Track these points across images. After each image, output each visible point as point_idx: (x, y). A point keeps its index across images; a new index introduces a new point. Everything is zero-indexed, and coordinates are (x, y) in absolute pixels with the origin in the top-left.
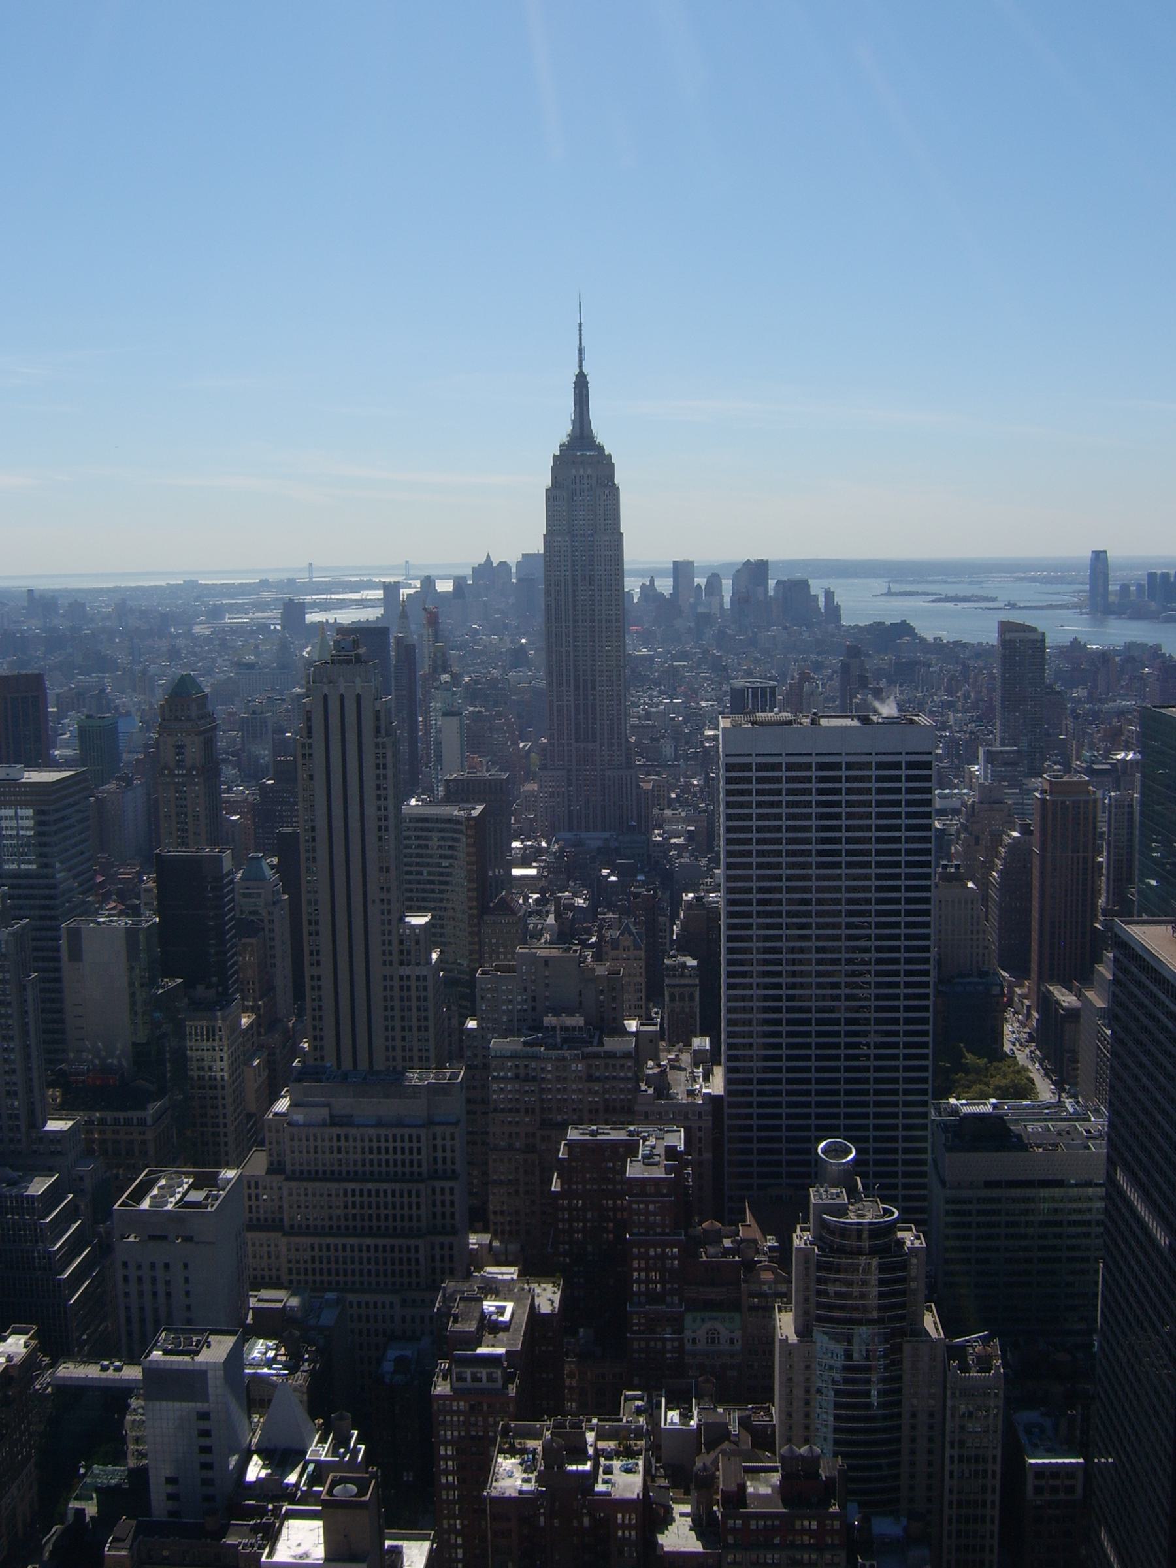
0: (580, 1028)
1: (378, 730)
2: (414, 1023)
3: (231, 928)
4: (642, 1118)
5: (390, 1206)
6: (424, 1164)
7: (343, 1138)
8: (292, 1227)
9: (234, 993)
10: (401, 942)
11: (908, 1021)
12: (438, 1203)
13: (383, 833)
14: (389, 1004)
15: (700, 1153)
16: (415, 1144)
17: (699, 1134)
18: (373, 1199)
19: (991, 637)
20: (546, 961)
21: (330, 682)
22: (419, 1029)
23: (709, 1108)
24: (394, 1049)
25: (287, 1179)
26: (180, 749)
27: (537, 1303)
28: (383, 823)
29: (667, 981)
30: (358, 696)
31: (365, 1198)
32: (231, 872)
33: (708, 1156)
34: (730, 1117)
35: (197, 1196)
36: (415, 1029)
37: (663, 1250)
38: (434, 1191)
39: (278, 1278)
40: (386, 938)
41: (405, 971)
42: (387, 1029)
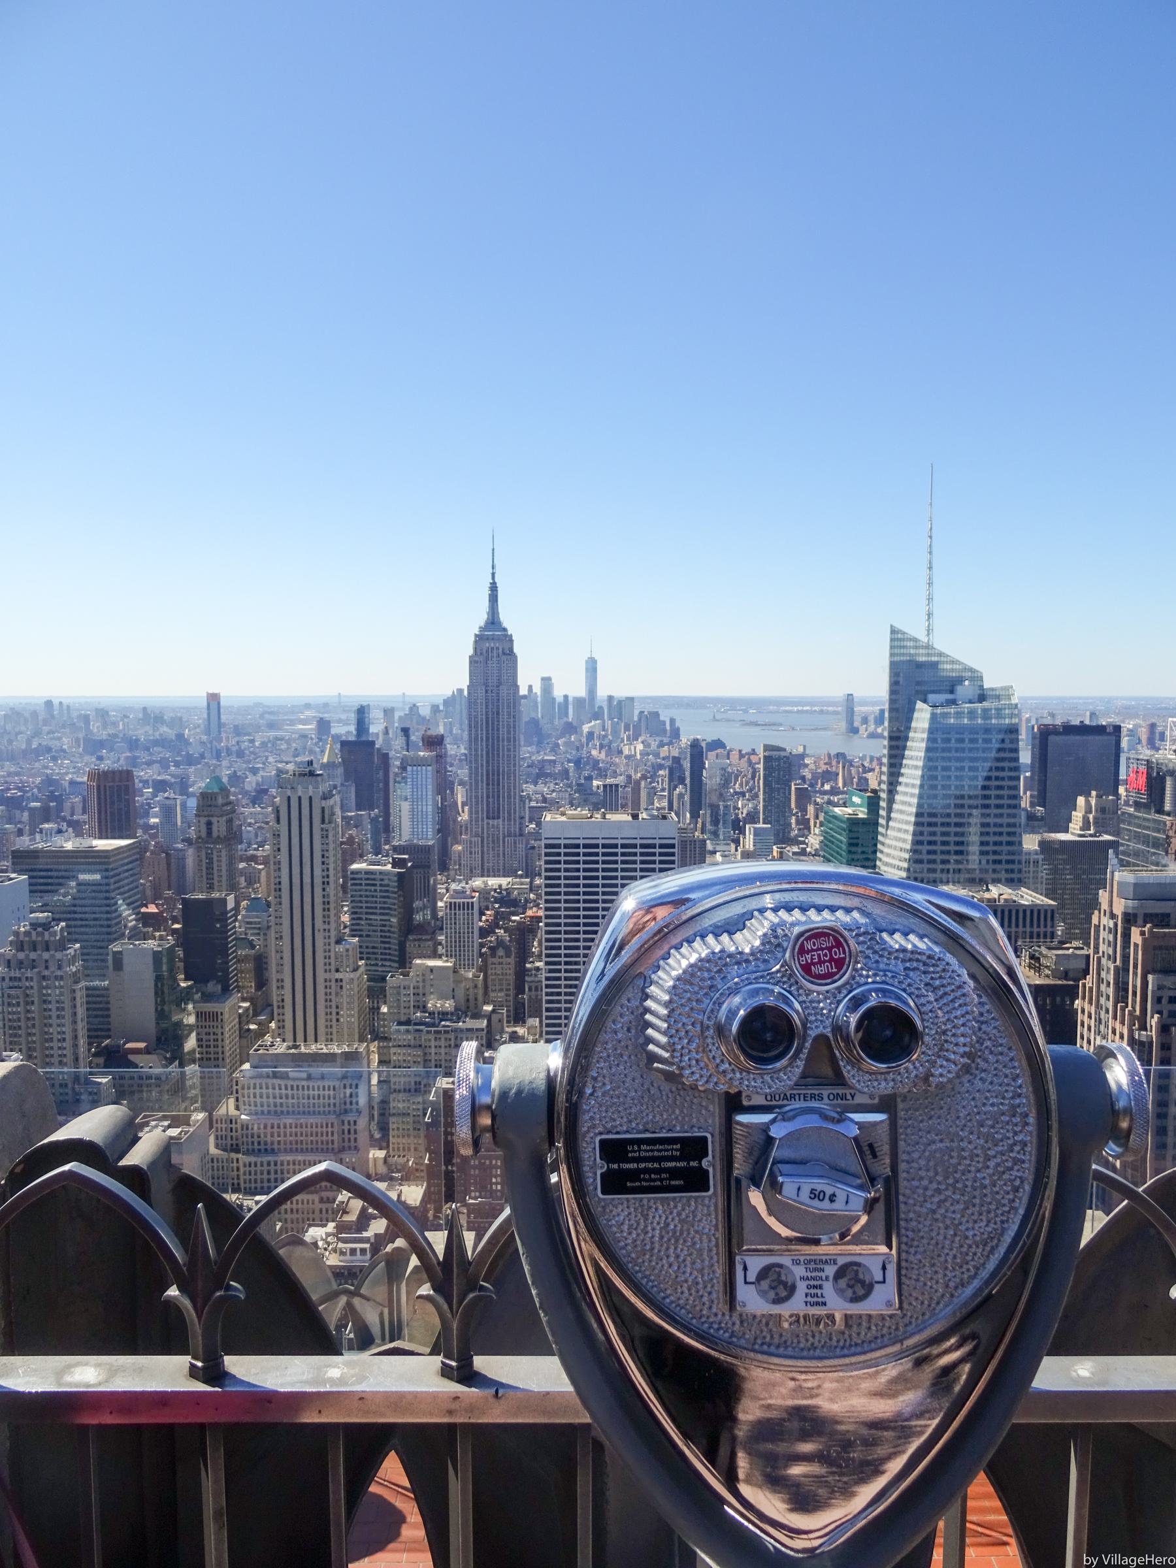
0: (452, 1014)
1: (323, 822)
3: (232, 947)
6: (337, 1105)
7: (283, 1087)
9: (233, 989)
13: (326, 886)
14: (328, 997)
20: (432, 970)
21: (292, 788)
24: (331, 1027)
26: (209, 824)
27: (403, 1199)
28: (326, 880)
29: (527, 978)
30: (311, 798)
32: (232, 910)
35: (173, 1132)
37: (491, 1162)
38: (343, 1122)
39: (239, 1184)
40: (327, 954)
41: (338, 976)
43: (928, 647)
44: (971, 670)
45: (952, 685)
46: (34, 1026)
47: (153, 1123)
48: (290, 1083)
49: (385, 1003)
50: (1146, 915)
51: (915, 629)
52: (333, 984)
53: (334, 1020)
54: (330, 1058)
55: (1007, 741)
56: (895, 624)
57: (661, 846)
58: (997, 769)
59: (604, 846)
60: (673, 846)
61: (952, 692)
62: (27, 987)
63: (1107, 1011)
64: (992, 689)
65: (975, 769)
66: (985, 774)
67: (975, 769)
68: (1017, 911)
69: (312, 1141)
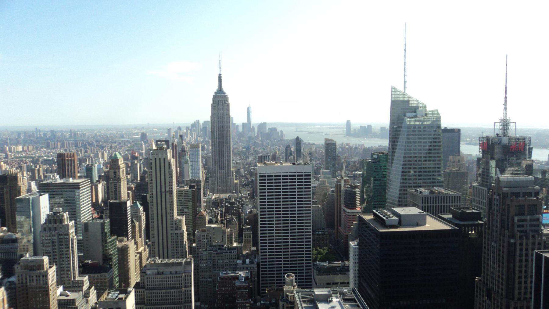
2: (179, 246)
4: (239, 269)
5: (174, 296)
6: (183, 284)
8: (147, 303)
10: (176, 224)
11: (306, 242)
12: (187, 294)
14: (173, 241)
15: (254, 278)
16: (180, 279)
17: (253, 273)
18: (169, 294)
19: (323, 143)
20: (214, 228)
22: (181, 247)
23: (256, 266)
25: (146, 290)
29: (244, 233)
31: (167, 294)
32: (129, 207)
33: (256, 279)
34: (262, 268)
35: (120, 296)
36: (179, 247)
41: (177, 232)
42: (172, 247)
43: (405, 94)
44: (422, 104)
45: (415, 110)
46: (56, 255)
47: (113, 293)
48: (163, 276)
49: (194, 243)
50: (511, 193)
51: (401, 88)
52: (174, 235)
53: (175, 250)
54: (180, 264)
55: (437, 131)
56: (393, 86)
57: (306, 175)
58: (434, 142)
59: (283, 176)
60: (310, 175)
61: (415, 112)
62: (53, 239)
63: (497, 231)
64: (430, 111)
65: (426, 142)
66: (429, 144)
67: (426, 142)
68: (449, 197)
69: (173, 299)
